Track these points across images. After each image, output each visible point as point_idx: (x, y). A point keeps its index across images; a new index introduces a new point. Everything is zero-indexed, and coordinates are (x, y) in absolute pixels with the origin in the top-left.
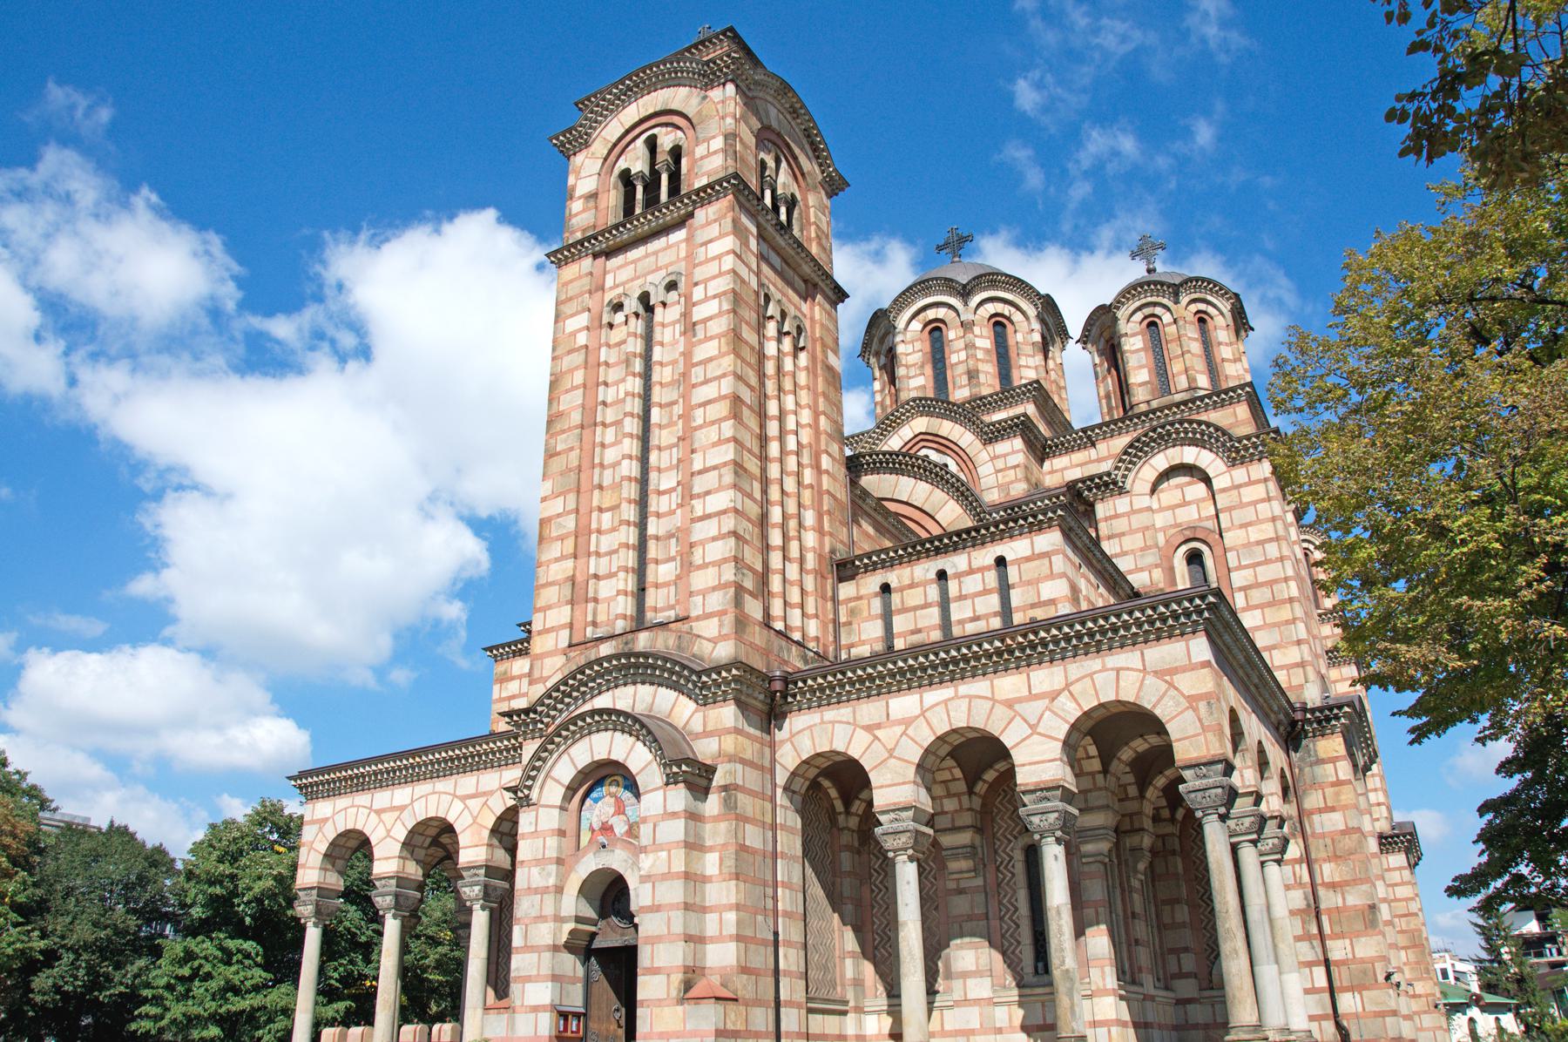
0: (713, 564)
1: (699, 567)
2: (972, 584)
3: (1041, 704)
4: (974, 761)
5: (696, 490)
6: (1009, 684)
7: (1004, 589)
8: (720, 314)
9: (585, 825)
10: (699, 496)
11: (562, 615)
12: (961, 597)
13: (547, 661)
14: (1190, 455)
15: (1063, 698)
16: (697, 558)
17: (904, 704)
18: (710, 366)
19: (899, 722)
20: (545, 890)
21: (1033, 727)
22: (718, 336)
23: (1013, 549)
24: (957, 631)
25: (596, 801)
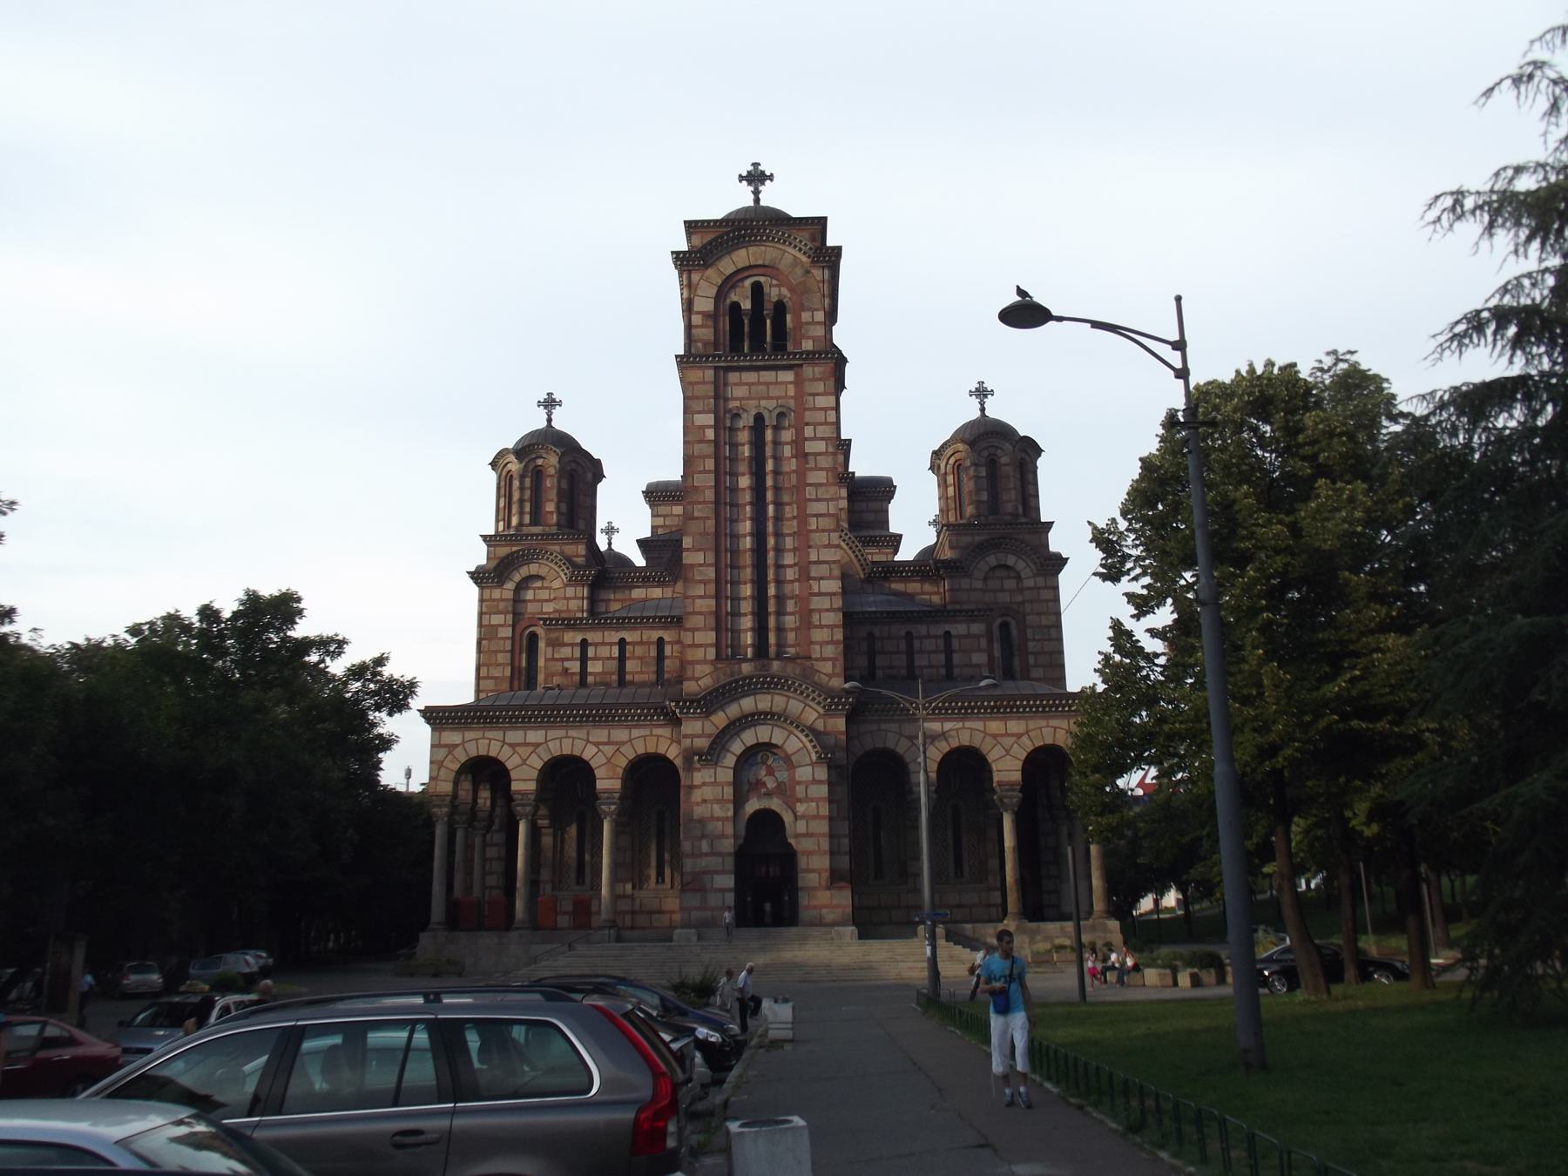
2: (929, 645)
3: (1013, 739)
4: (966, 767)
6: (995, 726)
8: (826, 453)
10: (814, 579)
12: (921, 652)
13: (698, 667)
14: (1011, 560)
15: (1024, 738)
18: (821, 490)
20: (727, 819)
21: (1008, 751)
22: (827, 470)
23: (959, 629)
24: (917, 672)
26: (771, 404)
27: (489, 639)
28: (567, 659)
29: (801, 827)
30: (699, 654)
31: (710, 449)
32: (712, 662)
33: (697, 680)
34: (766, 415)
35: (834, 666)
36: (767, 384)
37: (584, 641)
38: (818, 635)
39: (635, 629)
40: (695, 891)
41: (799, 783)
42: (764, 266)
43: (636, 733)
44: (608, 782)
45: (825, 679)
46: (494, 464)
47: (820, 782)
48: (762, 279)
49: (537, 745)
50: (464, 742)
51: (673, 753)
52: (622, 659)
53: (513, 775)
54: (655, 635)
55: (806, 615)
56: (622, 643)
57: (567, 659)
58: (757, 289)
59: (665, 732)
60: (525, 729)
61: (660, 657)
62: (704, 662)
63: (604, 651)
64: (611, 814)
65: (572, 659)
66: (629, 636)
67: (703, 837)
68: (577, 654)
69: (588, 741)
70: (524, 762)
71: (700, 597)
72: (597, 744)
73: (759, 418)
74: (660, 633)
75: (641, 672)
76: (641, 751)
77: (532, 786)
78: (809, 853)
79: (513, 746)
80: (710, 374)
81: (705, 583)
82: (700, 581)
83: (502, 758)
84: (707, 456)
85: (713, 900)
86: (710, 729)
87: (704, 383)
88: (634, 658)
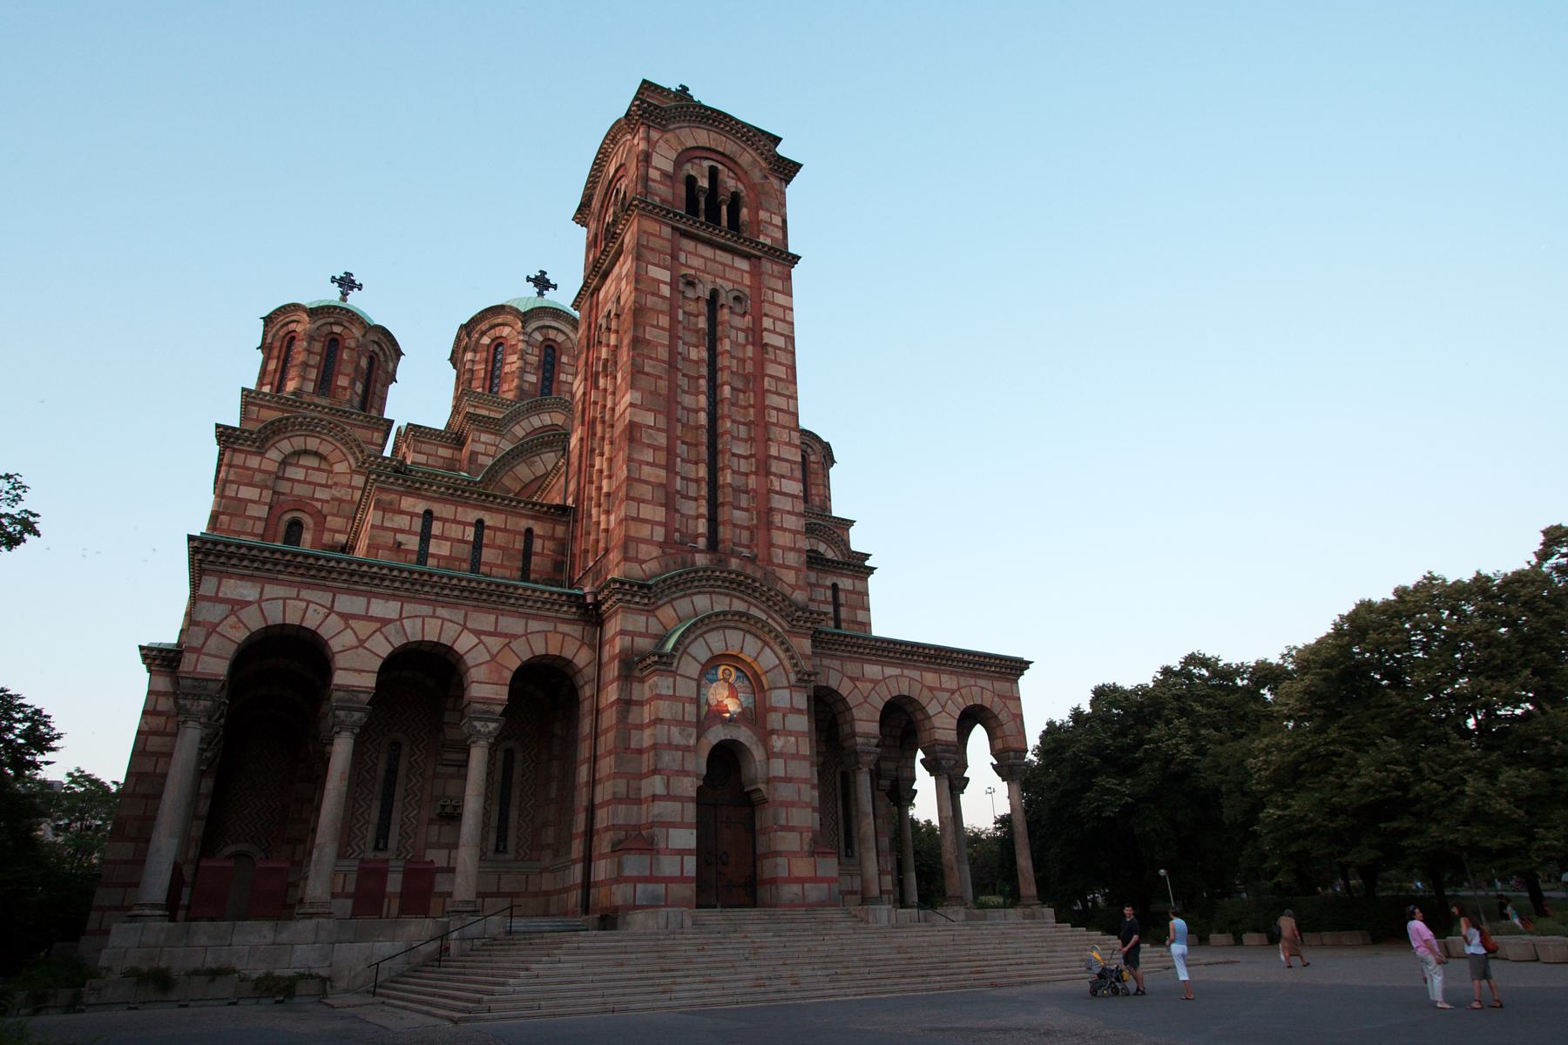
0: (790, 531)
1: (779, 528)
5: (773, 469)
6: (930, 678)
7: (837, 605)
9: (703, 701)
11: (660, 514)
13: (642, 546)
15: (957, 695)
16: (777, 519)
17: (872, 670)
18: (781, 384)
19: (871, 681)
20: (686, 749)
25: (712, 681)
26: (728, 286)
27: (231, 515)
28: (402, 531)
29: (778, 768)
30: (645, 531)
31: (665, 307)
32: (660, 545)
33: (642, 562)
34: (723, 294)
35: (797, 578)
36: (724, 265)
37: (428, 516)
38: (780, 538)
39: (499, 511)
40: (641, 851)
41: (775, 709)
42: (723, 154)
43: (534, 625)
44: (487, 686)
45: (788, 591)
46: (268, 320)
47: (799, 711)
48: (720, 167)
49: (385, 622)
50: (260, 600)
51: (582, 658)
52: (478, 545)
53: (340, 661)
54: (525, 524)
55: (766, 517)
56: (480, 524)
57: (402, 531)
58: (713, 174)
59: (575, 630)
60: (369, 595)
61: (527, 553)
62: (649, 542)
63: (455, 531)
64: (487, 735)
65: (410, 532)
66: (489, 519)
67: (655, 772)
68: (418, 525)
69: (464, 627)
70: (361, 643)
71: (648, 464)
72: (478, 633)
73: (714, 294)
74: (530, 523)
75: (502, 566)
76: (540, 650)
77: (370, 681)
78: (789, 805)
79: (346, 617)
80: (667, 231)
81: (655, 448)
82: (649, 446)
83: (324, 632)
84: (663, 312)
85: (669, 866)
86: (655, 627)
87: (660, 237)
88: (493, 546)
